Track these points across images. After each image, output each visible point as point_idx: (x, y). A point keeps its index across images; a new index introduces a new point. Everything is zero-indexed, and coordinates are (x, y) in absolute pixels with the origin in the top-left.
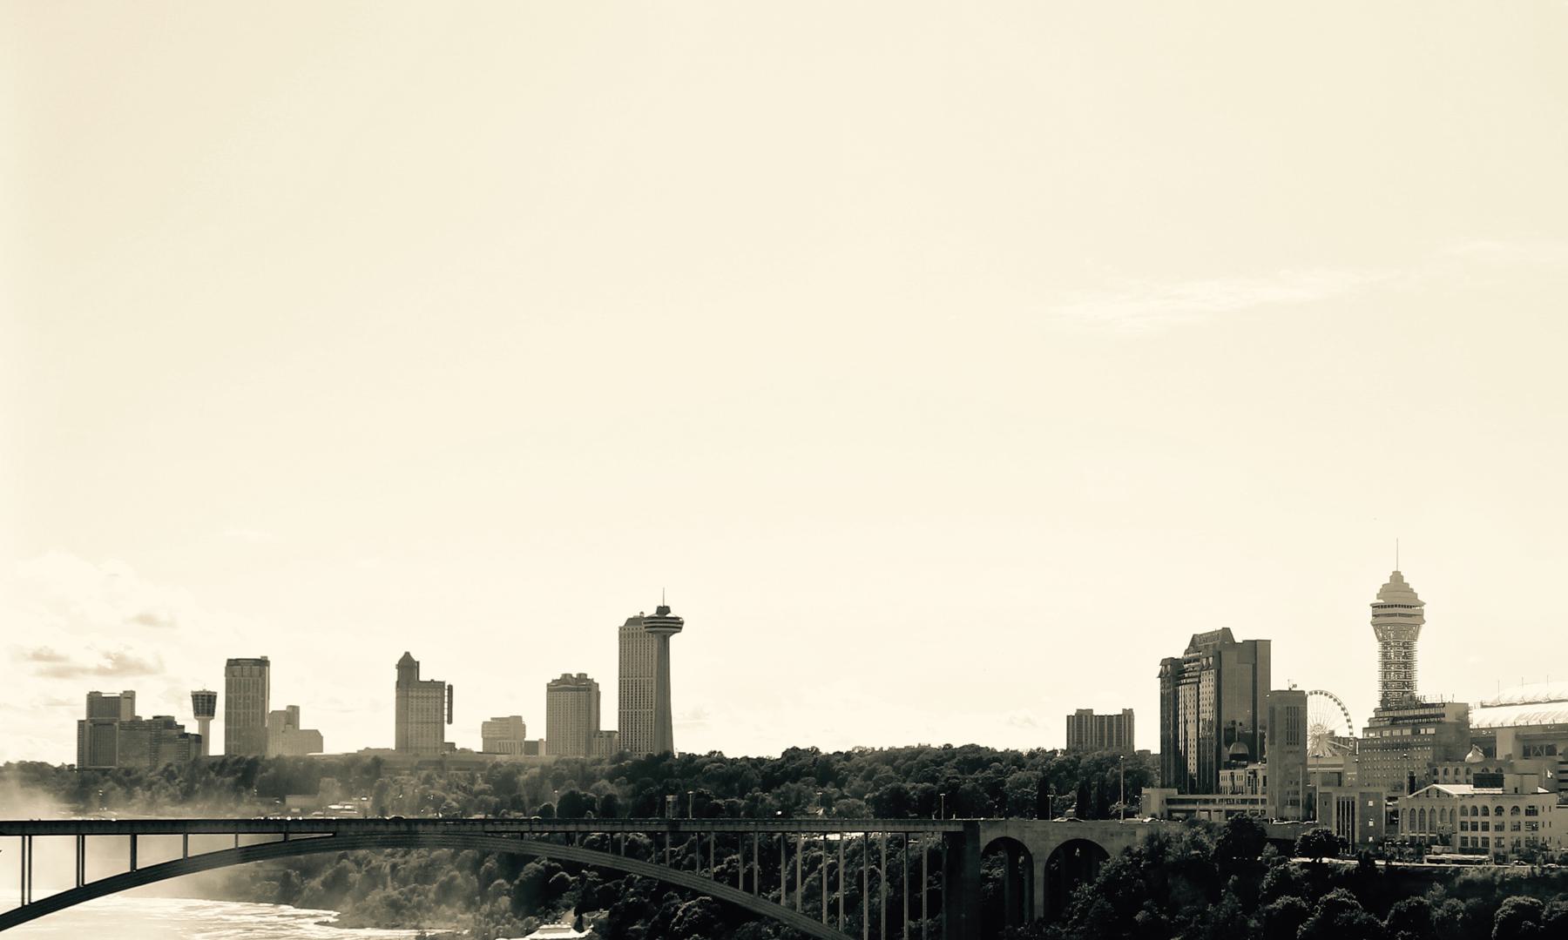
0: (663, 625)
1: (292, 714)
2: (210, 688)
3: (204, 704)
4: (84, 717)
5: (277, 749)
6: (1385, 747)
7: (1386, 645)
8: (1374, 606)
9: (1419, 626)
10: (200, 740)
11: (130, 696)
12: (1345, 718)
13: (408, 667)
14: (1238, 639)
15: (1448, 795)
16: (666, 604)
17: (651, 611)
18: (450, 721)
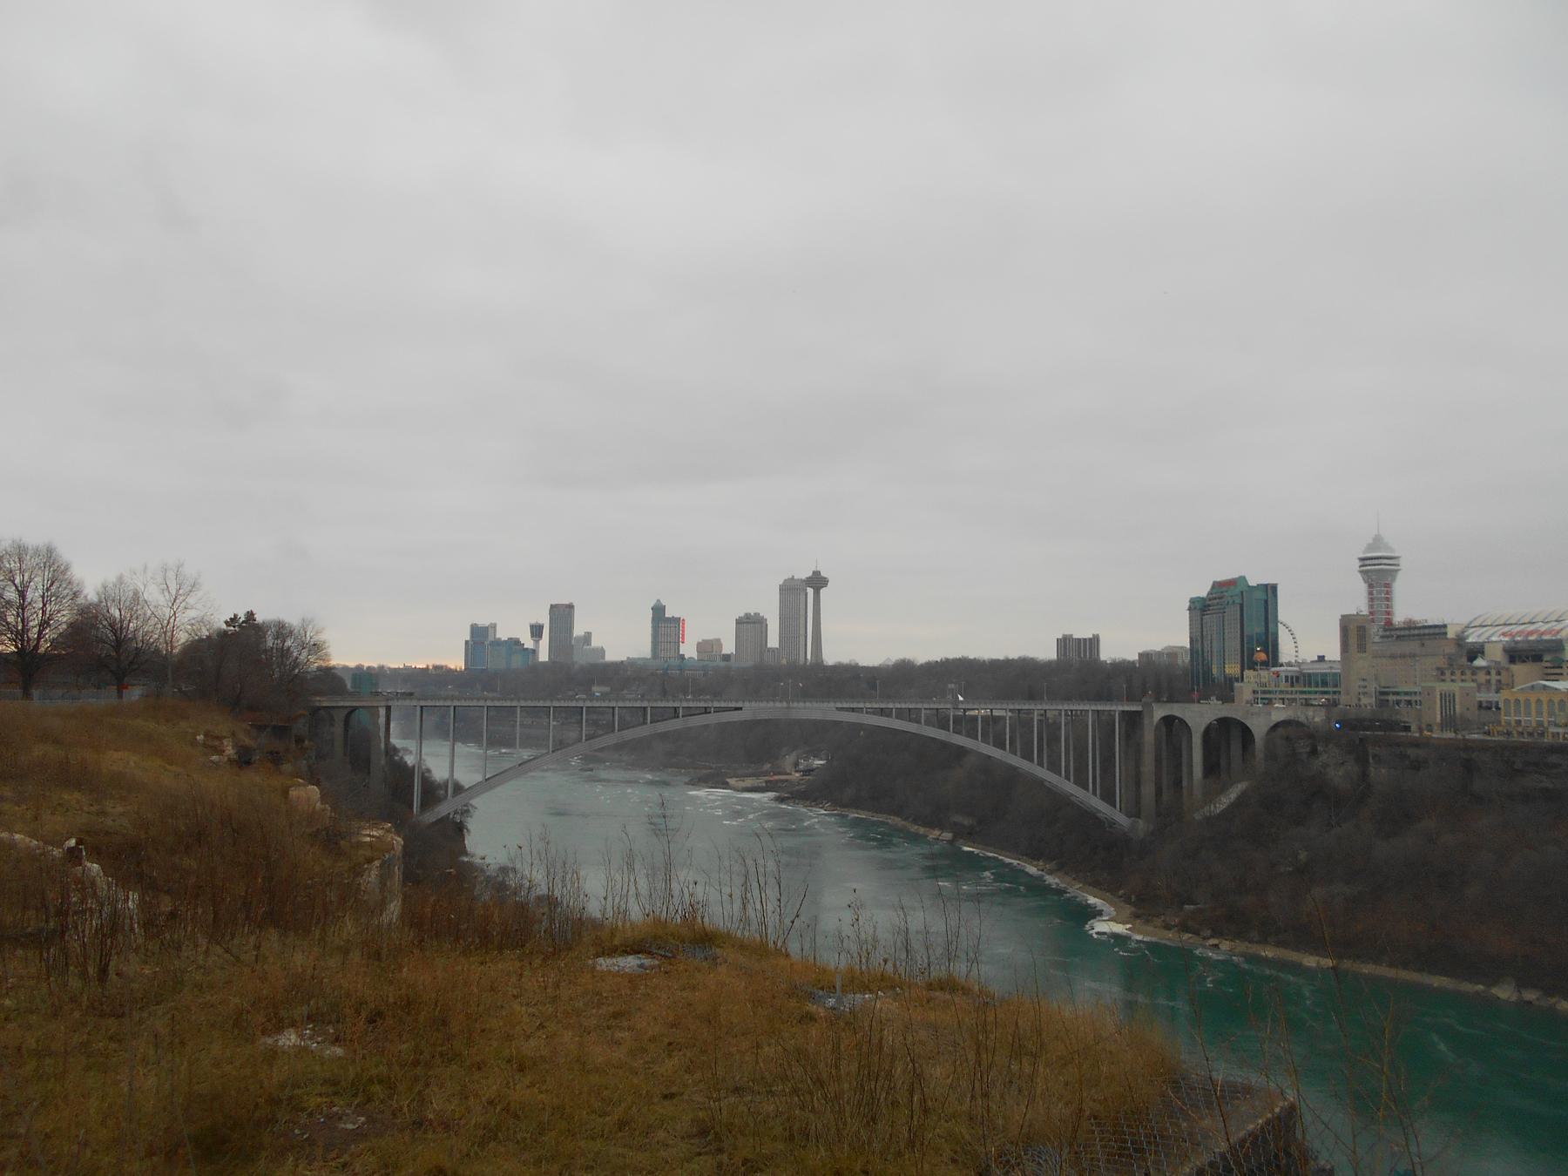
0: (818, 581)
1: (587, 638)
2: (540, 622)
3: (536, 631)
4: (468, 638)
5: (580, 659)
6: (1393, 657)
7: (1370, 586)
8: (1362, 559)
9: (1397, 571)
10: (534, 652)
11: (494, 626)
12: (1291, 637)
13: (658, 611)
14: (1252, 583)
15: (1559, 690)
16: (818, 569)
17: (810, 574)
18: (683, 642)
